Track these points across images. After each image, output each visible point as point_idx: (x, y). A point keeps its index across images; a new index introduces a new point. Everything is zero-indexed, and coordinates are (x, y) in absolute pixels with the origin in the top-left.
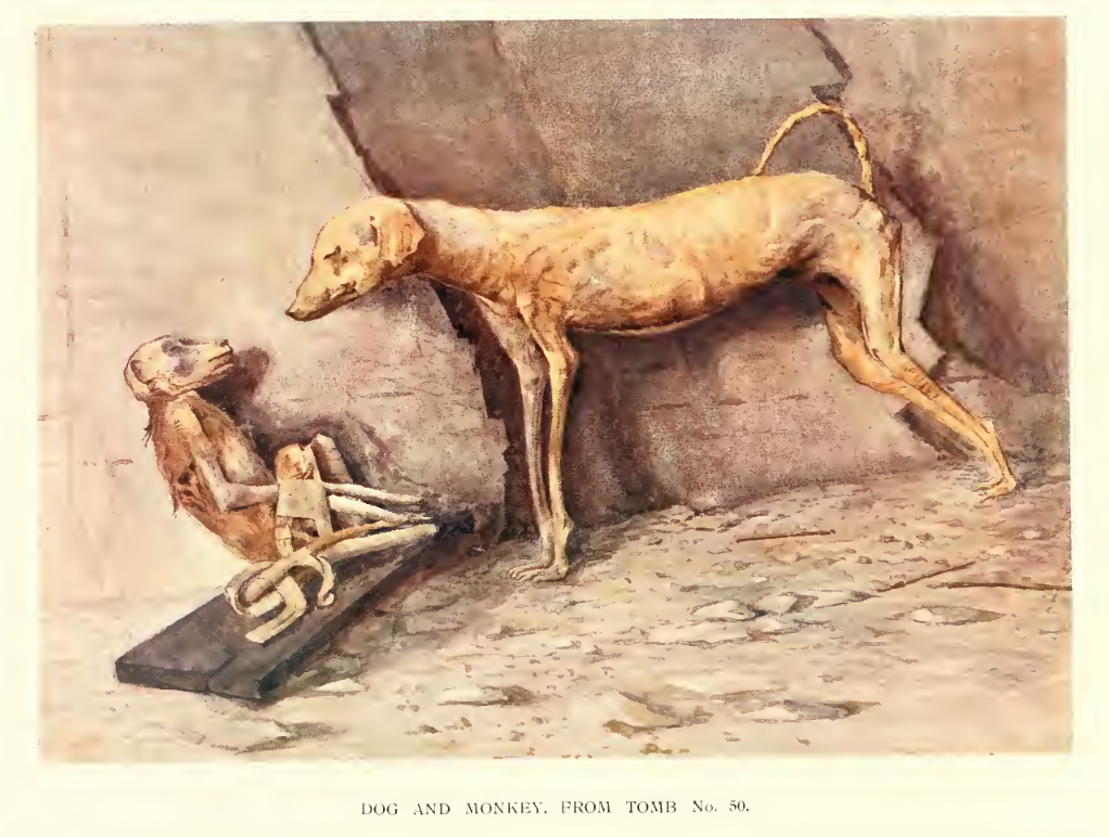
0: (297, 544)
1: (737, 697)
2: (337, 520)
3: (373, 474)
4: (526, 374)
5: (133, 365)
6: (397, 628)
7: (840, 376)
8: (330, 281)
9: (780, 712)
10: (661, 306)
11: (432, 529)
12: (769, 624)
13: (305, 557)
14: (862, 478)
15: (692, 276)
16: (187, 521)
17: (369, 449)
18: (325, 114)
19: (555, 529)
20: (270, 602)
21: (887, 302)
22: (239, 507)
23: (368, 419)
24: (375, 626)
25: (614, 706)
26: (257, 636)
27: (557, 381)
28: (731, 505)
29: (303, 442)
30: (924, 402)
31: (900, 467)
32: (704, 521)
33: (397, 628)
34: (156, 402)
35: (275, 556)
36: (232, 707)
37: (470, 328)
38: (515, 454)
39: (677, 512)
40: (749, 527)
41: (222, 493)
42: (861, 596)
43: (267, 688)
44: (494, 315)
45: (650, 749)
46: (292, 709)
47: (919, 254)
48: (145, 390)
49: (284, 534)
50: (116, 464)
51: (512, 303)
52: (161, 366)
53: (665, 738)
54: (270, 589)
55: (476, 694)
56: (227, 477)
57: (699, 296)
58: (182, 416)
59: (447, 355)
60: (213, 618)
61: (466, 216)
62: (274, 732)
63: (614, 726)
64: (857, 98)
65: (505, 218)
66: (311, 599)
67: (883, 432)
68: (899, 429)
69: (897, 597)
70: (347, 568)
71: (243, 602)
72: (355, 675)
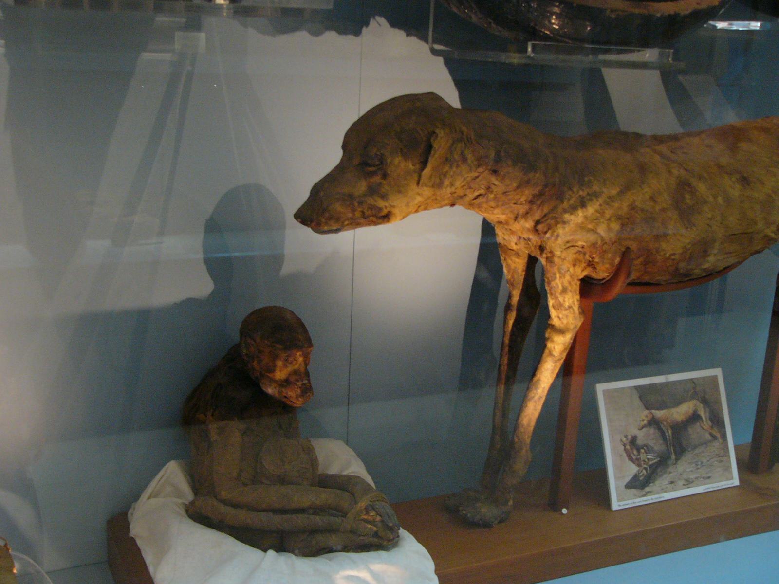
1: (697, 478)
2: (648, 459)
4: (667, 434)
8: (643, 423)
9: (702, 479)
11: (659, 459)
12: (699, 466)
13: (645, 466)
14: (706, 443)
16: (631, 463)
19: (673, 457)
22: (637, 459)
24: (655, 475)
26: (641, 479)
29: (643, 448)
30: (711, 431)
31: (710, 441)
34: (625, 445)
36: (639, 490)
37: (660, 429)
41: (634, 458)
42: (708, 461)
45: (688, 488)
46: (647, 489)
47: (707, 410)
48: (622, 443)
52: (624, 439)
53: (690, 485)
58: (628, 447)
59: (658, 434)
60: (636, 477)
62: (645, 493)
66: (647, 472)
67: (708, 437)
69: (713, 460)
70: (651, 466)
71: (639, 474)
72: (653, 483)
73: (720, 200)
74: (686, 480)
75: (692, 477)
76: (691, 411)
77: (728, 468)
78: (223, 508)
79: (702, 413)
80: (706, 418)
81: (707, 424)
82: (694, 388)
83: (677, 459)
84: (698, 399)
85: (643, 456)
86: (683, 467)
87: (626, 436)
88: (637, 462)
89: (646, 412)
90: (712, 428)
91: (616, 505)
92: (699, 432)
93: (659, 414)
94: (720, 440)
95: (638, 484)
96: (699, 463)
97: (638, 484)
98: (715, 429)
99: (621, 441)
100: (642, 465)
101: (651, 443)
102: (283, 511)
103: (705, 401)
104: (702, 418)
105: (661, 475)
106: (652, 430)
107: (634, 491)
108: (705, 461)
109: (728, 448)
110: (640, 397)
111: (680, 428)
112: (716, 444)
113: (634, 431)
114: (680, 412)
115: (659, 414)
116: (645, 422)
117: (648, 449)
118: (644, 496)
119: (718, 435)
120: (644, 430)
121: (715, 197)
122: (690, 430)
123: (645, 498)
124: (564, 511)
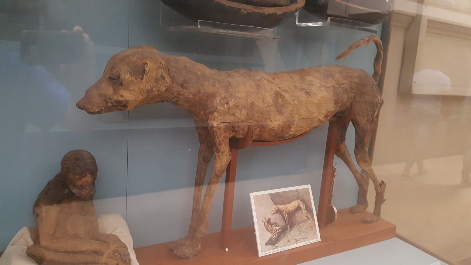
0: (274, 232)
1: (300, 238)
2: (276, 230)
3: (278, 226)
4: (285, 217)
5: (263, 220)
6: (281, 238)
7: (302, 214)
8: (273, 212)
9: (303, 239)
10: (292, 211)
11: (282, 230)
12: (301, 233)
13: (275, 233)
14: (304, 221)
15: (293, 208)
16: (268, 232)
17: (277, 224)
18: (271, 200)
19: (289, 228)
20: (274, 237)
21: (303, 208)
22: (271, 230)
23: (277, 222)
24: (280, 238)
25: (294, 241)
26: (273, 240)
27: (287, 217)
28: (298, 224)
29: (273, 225)
30: (307, 215)
31: (307, 220)
32: (297, 226)
33: (281, 238)
34: (265, 223)
35: (273, 233)
36: (272, 246)
37: (281, 214)
38: (286, 223)
39: (295, 226)
40: (299, 226)
41: (269, 229)
42: (306, 230)
43: (274, 244)
44: (283, 213)
45: (296, 243)
46: (276, 245)
47: (305, 205)
48: (263, 222)
49: (274, 232)
50: (263, 228)
51: (283, 212)
52: (264, 220)
53: (297, 242)
54: (273, 236)
55: (286, 241)
56: (270, 228)
57: (293, 210)
58: (266, 224)
59: (281, 217)
60: (271, 239)
61: (280, 206)
62: (275, 247)
63: (294, 242)
64: (299, 194)
65: (282, 206)
66: (276, 236)
67: (305, 218)
68: (306, 217)
69: (308, 229)
70: (278, 233)
71: (272, 238)
72: (279, 242)
73: (296, 102)
74: (295, 240)
76: (297, 206)
79: (302, 206)
80: (304, 208)
81: (304, 211)
82: (298, 194)
83: (291, 229)
84: (300, 200)
85: (274, 228)
86: (293, 233)
87: (265, 219)
88: (271, 231)
90: (307, 213)
91: (261, 254)
93: (281, 207)
94: (311, 219)
95: (271, 243)
96: (302, 231)
97: (271, 243)
98: (309, 214)
100: (274, 233)
101: (278, 222)
103: (303, 201)
104: (302, 209)
105: (283, 238)
106: (278, 215)
107: (270, 246)
109: (315, 223)
110: (272, 199)
111: (291, 214)
112: (309, 221)
113: (269, 216)
114: (291, 206)
115: (281, 207)
116: (274, 211)
117: (277, 226)
118: (275, 248)
119: (310, 217)
121: (293, 101)
122: (296, 215)
123: (275, 250)
124: (227, 250)
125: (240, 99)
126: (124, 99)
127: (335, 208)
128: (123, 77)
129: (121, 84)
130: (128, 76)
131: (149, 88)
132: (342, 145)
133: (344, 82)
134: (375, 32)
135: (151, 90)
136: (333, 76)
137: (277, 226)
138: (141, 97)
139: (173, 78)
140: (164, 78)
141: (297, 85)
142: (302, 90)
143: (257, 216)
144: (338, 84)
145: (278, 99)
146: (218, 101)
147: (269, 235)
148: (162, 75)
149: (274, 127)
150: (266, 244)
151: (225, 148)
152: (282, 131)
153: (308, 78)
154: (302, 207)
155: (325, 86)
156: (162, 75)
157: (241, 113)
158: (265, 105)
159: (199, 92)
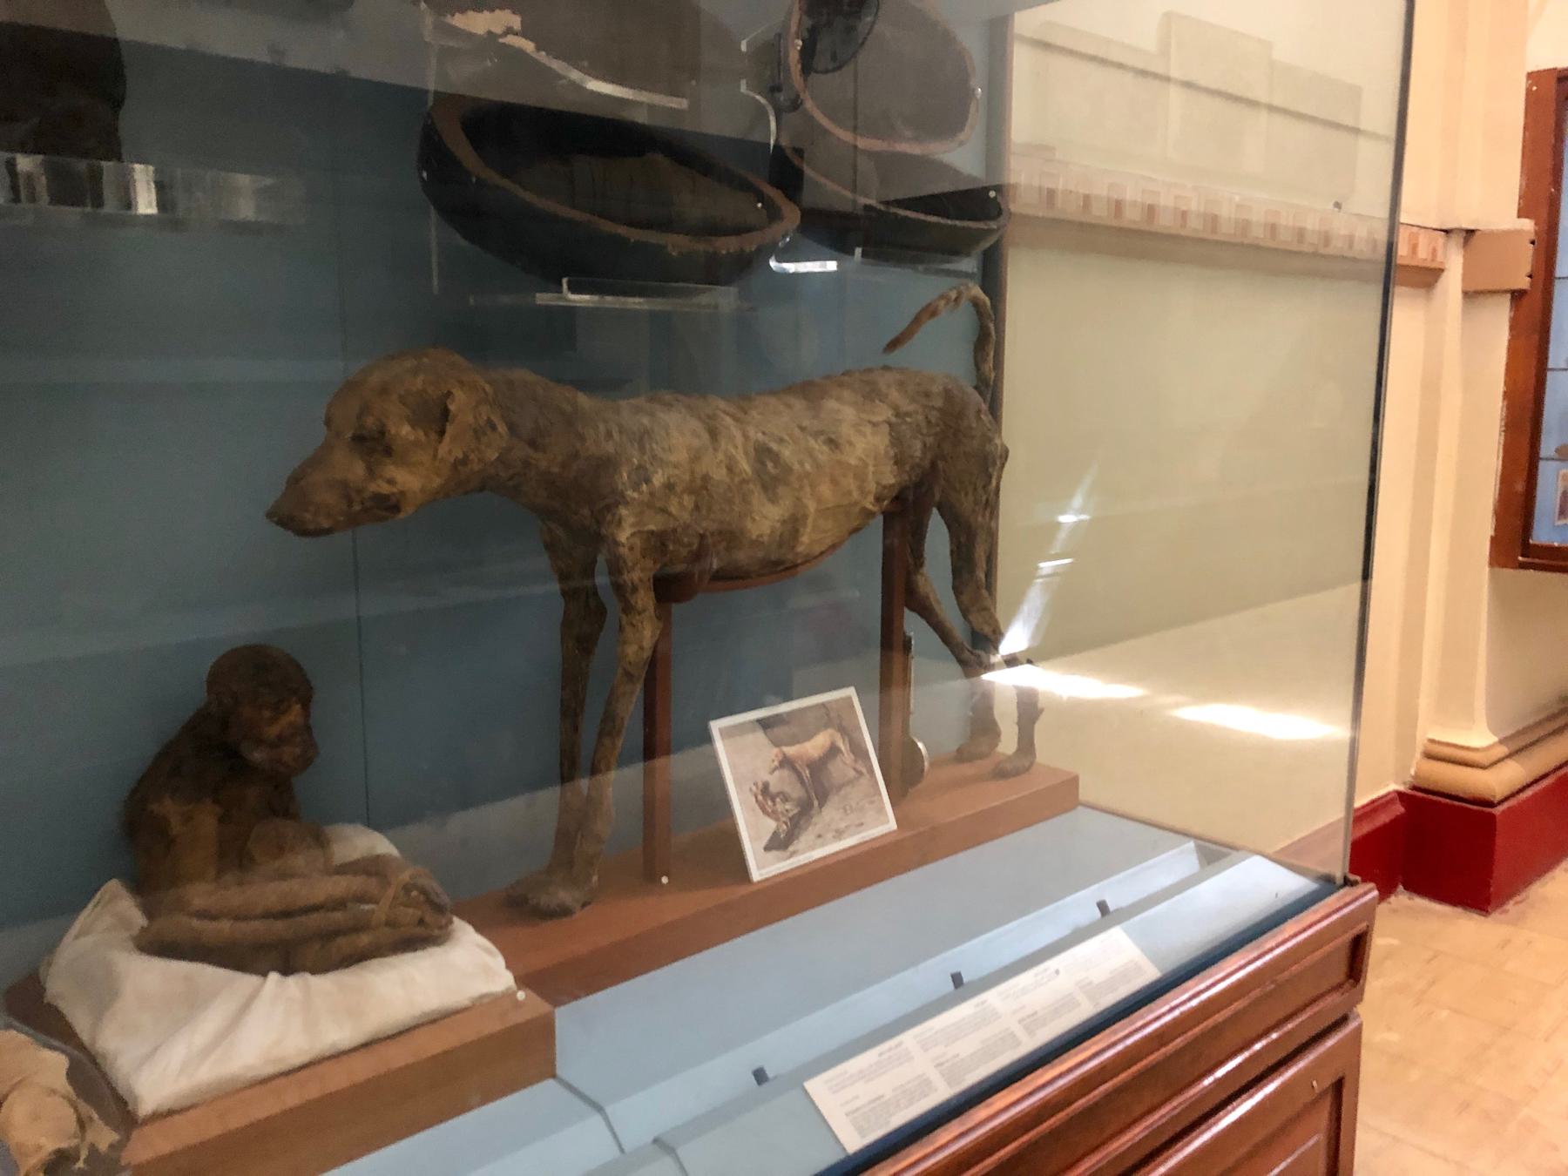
1: (846, 827)
8: (773, 766)
13: (784, 819)
14: (850, 782)
19: (816, 803)
22: (773, 811)
37: (794, 769)
38: (807, 791)
46: (791, 849)
52: (754, 788)
58: (760, 798)
59: (794, 777)
60: (775, 834)
67: (852, 774)
70: (790, 819)
75: (842, 825)
76: (828, 744)
77: (882, 810)
78: (195, 923)
80: (846, 749)
81: (848, 757)
82: (828, 715)
83: (821, 806)
85: (780, 807)
86: (829, 815)
87: (756, 784)
88: (772, 814)
89: (776, 750)
90: (856, 761)
91: (757, 875)
92: (842, 767)
93: (791, 751)
94: (868, 776)
95: (779, 843)
97: (779, 843)
98: (860, 762)
99: (751, 790)
101: (787, 789)
102: (286, 914)
103: (843, 730)
104: (842, 752)
105: (806, 829)
106: (786, 773)
107: (774, 853)
108: (854, 805)
111: (818, 767)
112: (864, 781)
114: (815, 746)
115: (791, 751)
116: (776, 763)
117: (786, 799)
119: (864, 770)
120: (777, 773)
125: (676, 466)
126: (395, 490)
127: (920, 745)
128: (393, 432)
129: (388, 452)
130: (406, 430)
131: (460, 456)
132: (919, 577)
133: (911, 408)
134: (967, 275)
135: (464, 461)
136: (883, 398)
137: (786, 799)
138: (437, 482)
139: (512, 428)
140: (494, 428)
141: (806, 423)
142: (817, 435)
143: (736, 781)
144: (897, 415)
145: (763, 464)
146: (625, 475)
147: (770, 825)
148: (489, 419)
149: (761, 536)
150: (767, 848)
151: (645, 599)
152: (780, 545)
153: (831, 404)
154: (843, 748)
155: (870, 422)
156: (489, 419)
157: (681, 504)
158: (737, 480)
159: (576, 455)
